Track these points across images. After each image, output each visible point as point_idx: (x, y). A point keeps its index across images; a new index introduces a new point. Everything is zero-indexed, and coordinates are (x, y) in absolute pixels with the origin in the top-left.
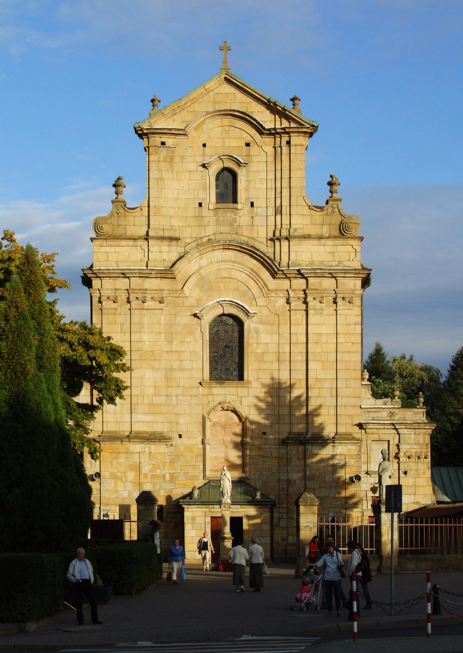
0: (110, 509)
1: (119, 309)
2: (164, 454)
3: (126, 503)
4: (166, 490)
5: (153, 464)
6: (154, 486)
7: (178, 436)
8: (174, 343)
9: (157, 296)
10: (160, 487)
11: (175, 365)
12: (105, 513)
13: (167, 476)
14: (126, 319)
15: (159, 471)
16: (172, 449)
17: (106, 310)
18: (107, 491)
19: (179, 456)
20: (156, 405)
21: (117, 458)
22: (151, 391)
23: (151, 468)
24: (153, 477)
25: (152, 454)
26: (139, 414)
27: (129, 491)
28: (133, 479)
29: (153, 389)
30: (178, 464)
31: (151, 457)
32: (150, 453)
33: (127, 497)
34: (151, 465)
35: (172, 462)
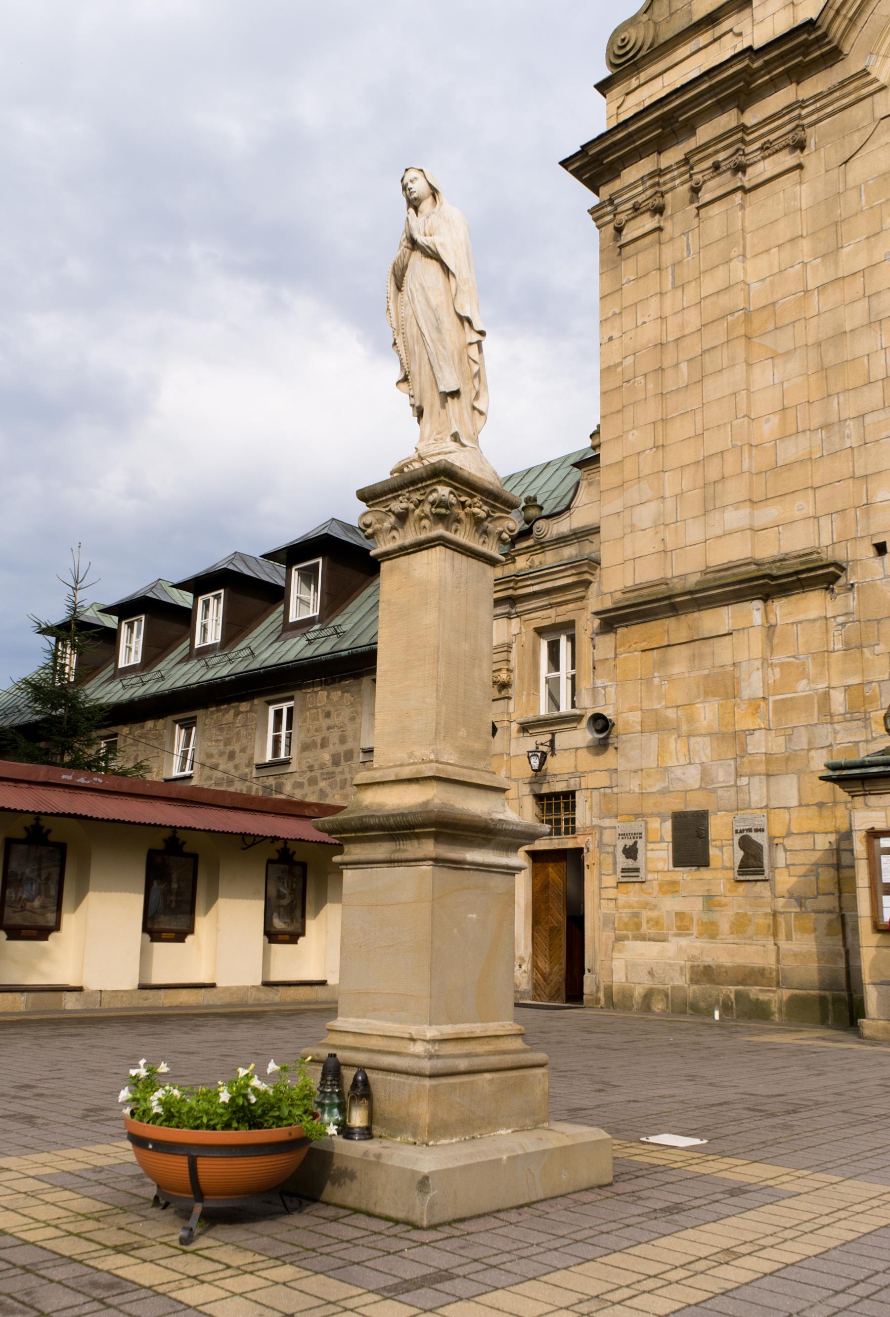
0: (642, 830)
1: (668, 226)
2: (818, 624)
3: (692, 808)
4: (836, 748)
5: (782, 665)
6: (789, 738)
7: (872, 552)
8: (846, 250)
9: (780, 133)
10: (810, 742)
11: (855, 316)
12: (630, 843)
13: (838, 702)
14: (688, 245)
15: (804, 682)
16: (852, 601)
17: (632, 246)
18: (635, 772)
19: (878, 621)
20: (788, 466)
21: (663, 663)
22: (768, 429)
23: (778, 676)
24: (783, 707)
25: (778, 629)
26: (730, 508)
27: (702, 764)
28: (715, 725)
29: (775, 419)
30: (878, 649)
31: (776, 641)
32: (770, 629)
33: (697, 786)
34: (777, 670)
35: (854, 647)
